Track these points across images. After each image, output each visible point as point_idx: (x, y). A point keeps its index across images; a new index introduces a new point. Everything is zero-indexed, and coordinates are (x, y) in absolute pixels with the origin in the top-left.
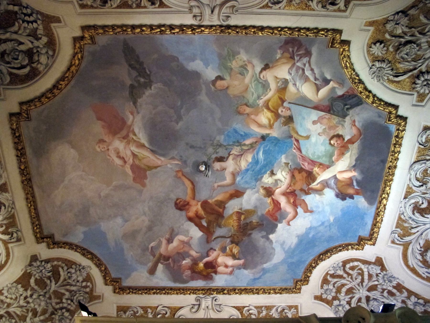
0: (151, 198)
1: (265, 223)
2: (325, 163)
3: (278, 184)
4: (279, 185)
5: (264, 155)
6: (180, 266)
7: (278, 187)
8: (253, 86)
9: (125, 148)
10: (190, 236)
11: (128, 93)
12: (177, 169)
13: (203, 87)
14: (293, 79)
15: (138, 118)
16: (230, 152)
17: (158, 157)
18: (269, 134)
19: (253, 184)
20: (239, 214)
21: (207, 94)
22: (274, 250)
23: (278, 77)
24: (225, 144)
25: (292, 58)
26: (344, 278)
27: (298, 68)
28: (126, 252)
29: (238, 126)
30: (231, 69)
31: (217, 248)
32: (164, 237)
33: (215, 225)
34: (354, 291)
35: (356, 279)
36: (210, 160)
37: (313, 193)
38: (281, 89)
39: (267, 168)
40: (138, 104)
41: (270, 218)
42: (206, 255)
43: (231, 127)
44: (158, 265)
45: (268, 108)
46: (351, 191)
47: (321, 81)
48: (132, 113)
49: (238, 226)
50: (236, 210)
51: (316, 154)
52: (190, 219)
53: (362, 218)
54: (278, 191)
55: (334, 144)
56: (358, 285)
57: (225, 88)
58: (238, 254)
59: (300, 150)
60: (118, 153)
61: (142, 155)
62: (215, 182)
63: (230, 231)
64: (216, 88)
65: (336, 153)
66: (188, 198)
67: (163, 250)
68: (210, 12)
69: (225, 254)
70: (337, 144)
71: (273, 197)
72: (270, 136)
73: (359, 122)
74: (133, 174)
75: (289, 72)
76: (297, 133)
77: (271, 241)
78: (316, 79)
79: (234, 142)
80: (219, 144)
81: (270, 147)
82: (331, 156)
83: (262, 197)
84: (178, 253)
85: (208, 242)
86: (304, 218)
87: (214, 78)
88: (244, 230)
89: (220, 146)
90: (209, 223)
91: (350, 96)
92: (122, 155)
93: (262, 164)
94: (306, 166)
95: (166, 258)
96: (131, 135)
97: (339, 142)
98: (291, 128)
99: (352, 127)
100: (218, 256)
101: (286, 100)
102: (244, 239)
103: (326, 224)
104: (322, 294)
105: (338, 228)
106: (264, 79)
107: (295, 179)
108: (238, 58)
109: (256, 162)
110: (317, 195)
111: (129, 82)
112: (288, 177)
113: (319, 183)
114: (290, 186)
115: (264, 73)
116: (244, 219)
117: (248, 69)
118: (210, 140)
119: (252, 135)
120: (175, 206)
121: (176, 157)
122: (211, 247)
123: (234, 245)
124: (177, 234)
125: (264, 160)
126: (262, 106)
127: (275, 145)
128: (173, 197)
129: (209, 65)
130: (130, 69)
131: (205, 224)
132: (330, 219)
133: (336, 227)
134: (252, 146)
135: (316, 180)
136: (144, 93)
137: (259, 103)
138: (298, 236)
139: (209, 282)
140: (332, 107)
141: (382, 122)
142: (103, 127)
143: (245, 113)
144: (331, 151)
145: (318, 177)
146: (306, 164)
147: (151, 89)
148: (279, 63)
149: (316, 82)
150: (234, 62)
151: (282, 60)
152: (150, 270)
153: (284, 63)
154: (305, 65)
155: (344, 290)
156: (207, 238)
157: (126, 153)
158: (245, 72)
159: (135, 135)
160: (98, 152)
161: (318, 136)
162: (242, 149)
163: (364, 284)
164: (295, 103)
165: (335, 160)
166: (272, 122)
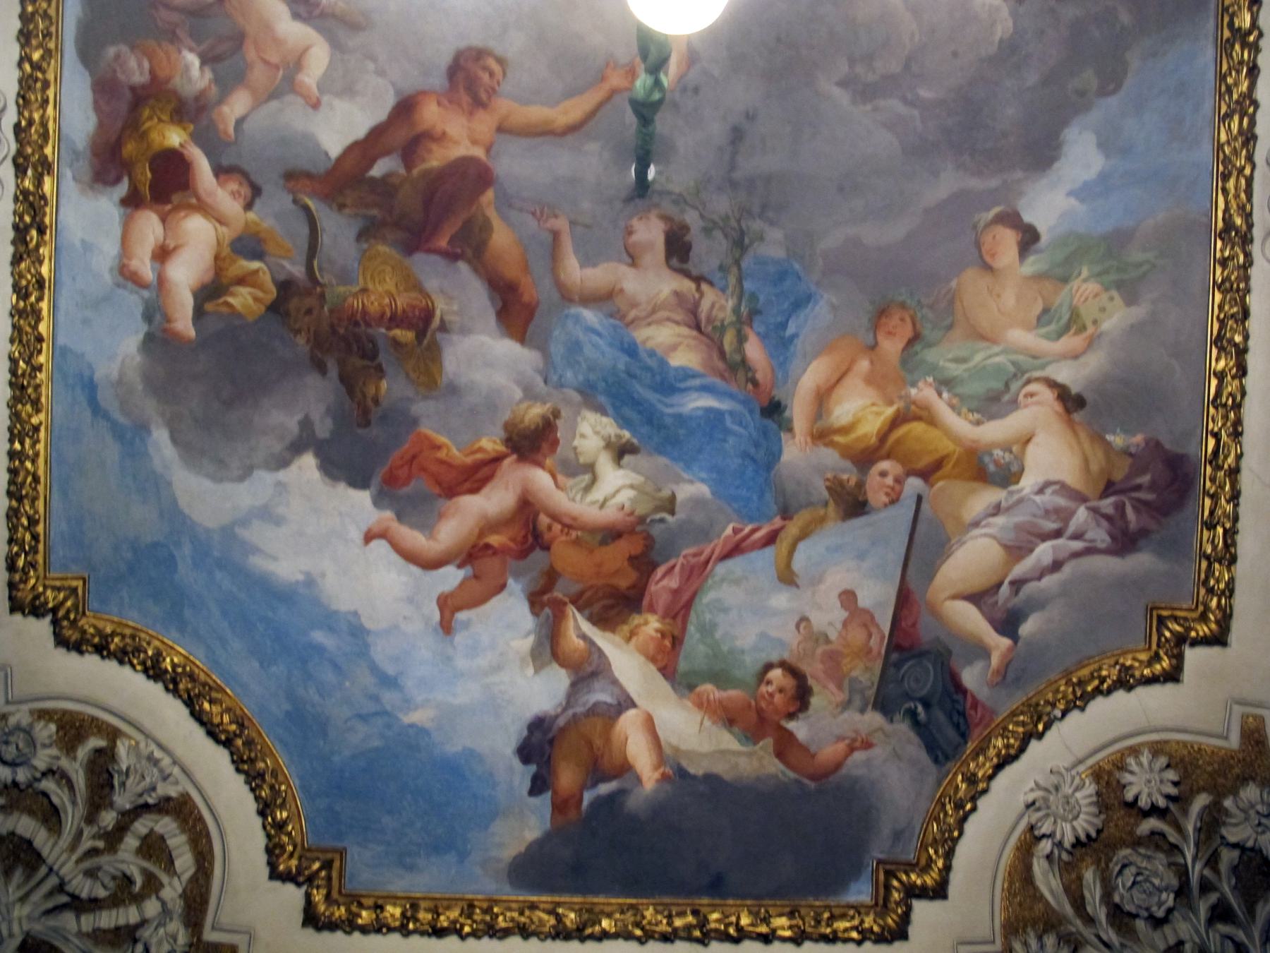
1: (375, 431)
4: (570, 482)
5: (700, 413)
6: (173, 38)
7: (560, 477)
8: (997, 359)
13: (994, 183)
14: (1020, 501)
16: (711, 284)
18: (790, 430)
19: (569, 374)
20: (422, 321)
22: (241, 479)
23: (1031, 448)
24: (746, 263)
25: (1109, 488)
26: (91, 819)
27: (1064, 515)
30: (1065, 280)
31: (262, 218)
33: (375, 212)
34: (18, 875)
35: (91, 874)
36: (675, 202)
38: (980, 460)
39: (645, 430)
42: (225, 162)
43: (818, 284)
45: (896, 422)
46: (567, 777)
47: (1010, 605)
49: (365, 312)
50: (440, 306)
52: (405, 108)
53: (438, 847)
54: (540, 479)
55: (769, 683)
56: (61, 888)
57: (988, 259)
59: (735, 550)
62: (573, 223)
63: (345, 277)
65: (733, 693)
66: (503, 105)
69: (226, 251)
70: (771, 695)
71: (507, 462)
73: (868, 763)
75: (1048, 484)
76: (804, 535)
77: (282, 463)
78: (1017, 584)
79: (753, 297)
80: (747, 241)
81: (735, 434)
82: (720, 678)
83: (507, 416)
84: (239, 39)
85: (291, 176)
86: (410, 600)
87: (1027, 218)
89: (740, 243)
90: (385, 187)
91: (962, 714)
93: (660, 406)
94: (665, 582)
97: (778, 698)
98: (822, 512)
100: (221, 220)
102: (301, 340)
103: (389, 698)
105: (377, 749)
106: (1021, 397)
107: (604, 543)
108: (1112, 299)
109: (669, 383)
110: (531, 640)
112: (610, 515)
113: (591, 643)
114: (568, 527)
115: (1048, 395)
116: (396, 343)
117: (1064, 339)
118: (764, 207)
119: (782, 365)
120: (470, 49)
122: (267, 189)
123: (273, 292)
124: (336, 45)
127: (745, 455)
129: (1082, 201)
131: (377, 171)
132: (416, 708)
133: (377, 743)
134: (738, 367)
137: (921, 384)
138: (310, 582)
139: (84, 166)
140: (913, 657)
141: (878, 850)
143: (881, 338)
144: (738, 673)
145: (617, 638)
146: (673, 582)
148: (1087, 446)
149: (1005, 589)
150: (1092, 287)
153: (1086, 461)
154: (1077, 536)
155: (25, 825)
156: (309, 175)
158: (1053, 327)
161: (796, 619)
162: (722, 329)
163: (68, 921)
164: (922, 516)
165: (699, 695)
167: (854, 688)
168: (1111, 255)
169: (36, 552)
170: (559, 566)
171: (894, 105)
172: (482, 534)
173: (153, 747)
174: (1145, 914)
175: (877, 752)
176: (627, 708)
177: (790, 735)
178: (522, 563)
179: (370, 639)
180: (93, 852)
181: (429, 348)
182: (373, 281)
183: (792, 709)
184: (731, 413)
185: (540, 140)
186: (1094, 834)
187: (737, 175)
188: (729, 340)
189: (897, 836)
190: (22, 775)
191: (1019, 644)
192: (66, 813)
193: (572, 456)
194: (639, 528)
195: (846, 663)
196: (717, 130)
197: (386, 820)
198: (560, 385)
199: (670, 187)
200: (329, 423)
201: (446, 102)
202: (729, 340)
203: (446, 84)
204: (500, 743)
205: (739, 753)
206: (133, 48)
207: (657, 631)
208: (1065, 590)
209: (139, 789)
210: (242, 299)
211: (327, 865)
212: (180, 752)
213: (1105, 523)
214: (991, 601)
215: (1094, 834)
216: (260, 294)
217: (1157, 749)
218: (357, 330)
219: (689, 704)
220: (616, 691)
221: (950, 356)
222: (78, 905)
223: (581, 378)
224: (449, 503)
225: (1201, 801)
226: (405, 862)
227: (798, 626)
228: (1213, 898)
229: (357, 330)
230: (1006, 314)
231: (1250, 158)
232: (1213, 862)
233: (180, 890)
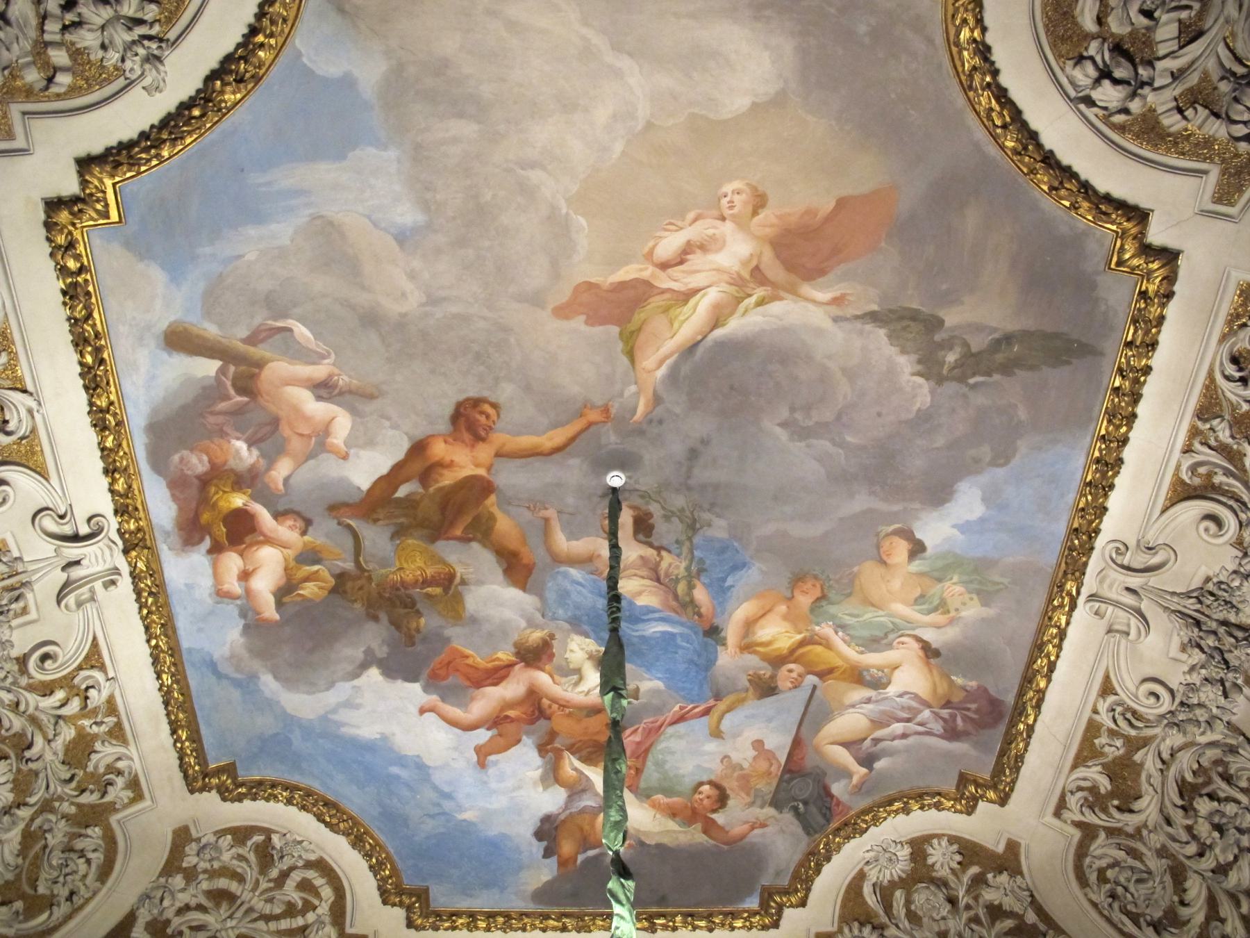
0: (506, 329)
1: (419, 647)
3: (566, 676)
4: (564, 680)
6: (223, 434)
7: (556, 677)
10: (352, 451)
12: (613, 411)
13: (896, 508)
15: (819, 317)
16: (669, 551)
17: (669, 362)
18: (724, 645)
20: (448, 581)
21: (870, 511)
22: (328, 689)
23: (897, 673)
24: (697, 539)
25: (948, 704)
28: (252, 231)
29: (753, 575)
30: (940, 580)
32: (336, 371)
33: (402, 520)
35: (270, 900)
36: (642, 497)
37: (546, 763)
40: (868, 327)
41: (438, 659)
42: (281, 508)
44: (212, 357)
45: (802, 643)
46: (567, 848)
48: (837, 301)
49: (403, 582)
50: (460, 571)
51: (668, 758)
52: (418, 448)
53: (487, 885)
54: (542, 678)
57: (885, 558)
58: (299, 599)
59: (681, 719)
60: (703, 248)
61: (682, 318)
63: (384, 563)
64: (888, 535)
65: (675, 799)
66: (500, 438)
67: (278, 368)
69: (292, 564)
71: (517, 667)
72: (719, 648)
73: (763, 835)
74: (611, 284)
75: (906, 693)
76: (730, 709)
77: (355, 675)
78: (876, 741)
79: (701, 561)
80: (698, 526)
81: (683, 648)
82: (667, 792)
83: (516, 637)
84: (275, 422)
85: (334, 508)
86: (456, 749)
87: (918, 535)
88: (389, 599)
89: (693, 527)
90: (410, 503)
91: (830, 809)
92: (696, 260)
93: (628, 631)
96: (760, 292)
100: (282, 545)
102: (358, 606)
103: (447, 805)
104: (198, 840)
107: (588, 716)
110: (540, 771)
111: (952, 318)
113: (582, 773)
116: (429, 596)
119: (721, 604)
120: (467, 400)
121: (659, 410)
123: (332, 582)
124: (353, 411)
125: (642, 638)
126: (813, 630)
127: (691, 662)
128: (506, 393)
129: (962, 533)
130: (996, 336)
131: (402, 492)
133: (442, 830)
134: (688, 605)
139: (175, 539)
142: (810, 212)
143: (797, 593)
146: (637, 738)
147: (913, 374)
148: (937, 679)
149: (868, 742)
150: (958, 589)
151: (945, 685)
152: (186, 330)
156: (346, 505)
157: (698, 271)
159: (761, 303)
160: (720, 186)
162: (677, 581)
163: (261, 925)
164: (815, 697)
166: (758, 649)
167: (758, 794)
171: (823, 445)
172: (502, 709)
177: (713, 821)
178: (533, 727)
179: (431, 771)
184: (681, 635)
187: (691, 482)
189: (778, 874)
193: (564, 663)
196: (677, 448)
198: (554, 619)
199: (637, 487)
200: (385, 649)
201: (450, 440)
202: (681, 588)
204: (523, 831)
206: (192, 450)
208: (907, 750)
213: (941, 722)
214: (856, 747)
217: (952, 840)
223: (569, 614)
224: (477, 692)
225: (974, 870)
226: (466, 892)
228: (972, 913)
229: (399, 593)
230: (893, 590)
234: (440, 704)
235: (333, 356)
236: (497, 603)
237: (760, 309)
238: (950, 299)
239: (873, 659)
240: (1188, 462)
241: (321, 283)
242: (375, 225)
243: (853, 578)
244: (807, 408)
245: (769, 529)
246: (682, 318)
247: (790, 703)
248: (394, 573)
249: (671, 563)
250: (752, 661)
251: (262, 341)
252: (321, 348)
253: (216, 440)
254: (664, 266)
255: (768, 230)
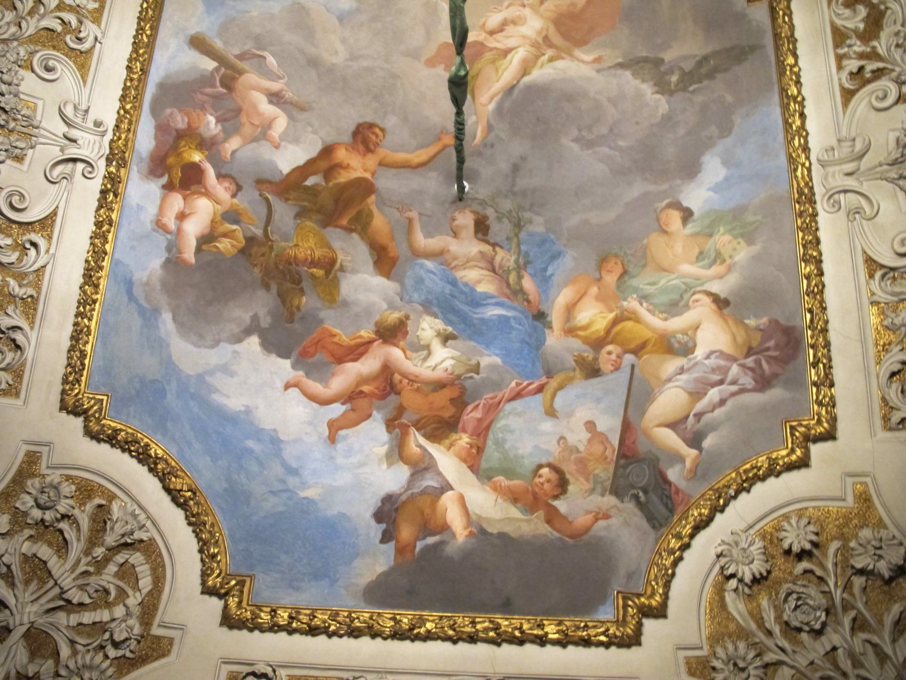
0: (395, 76)
1: (296, 326)
2: (483, 458)
3: (417, 351)
4: (414, 355)
6: (203, 108)
7: (408, 352)
9: (524, 37)
10: (283, 144)
11: (644, 54)
13: (665, 187)
14: (696, 364)
15: (587, 71)
16: (502, 247)
17: (497, 99)
18: (551, 328)
19: (416, 296)
20: (330, 265)
21: (646, 195)
22: (212, 347)
24: (523, 235)
26: (87, 552)
27: (725, 371)
29: (567, 262)
30: (711, 235)
32: (286, 88)
33: (305, 204)
34: (33, 586)
35: (82, 588)
36: (480, 204)
38: (669, 342)
39: (462, 326)
40: (620, 72)
42: (223, 172)
43: (565, 246)
44: (214, 59)
45: (615, 322)
46: (406, 532)
47: (695, 429)
48: (598, 60)
49: (296, 257)
50: (341, 257)
52: (327, 151)
53: (317, 576)
54: (396, 353)
55: (540, 476)
58: (215, 250)
59: (517, 395)
60: (514, 22)
61: (503, 67)
63: (286, 238)
64: (662, 210)
66: (382, 152)
67: (251, 78)
68: (846, 172)
69: (219, 218)
70: (542, 484)
71: (376, 343)
72: (547, 331)
73: (608, 528)
76: (561, 387)
77: (239, 340)
78: (699, 416)
79: (527, 254)
80: (522, 224)
81: (517, 330)
82: (509, 473)
83: (378, 317)
84: (238, 111)
85: (260, 182)
86: (310, 423)
87: (685, 204)
88: (283, 272)
89: (518, 225)
90: (313, 191)
91: (669, 497)
92: (510, 29)
93: (471, 314)
94: (472, 414)
95: (229, 83)
96: (550, 53)
98: (572, 374)
99: (591, 512)
101: (639, 358)
102: (257, 270)
103: (292, 481)
106: (690, 303)
107: (435, 390)
108: (739, 243)
109: (477, 301)
110: (386, 447)
111: (668, 56)
112: (439, 374)
113: (425, 450)
116: (313, 276)
117: (714, 267)
118: (532, 205)
120: (365, 123)
121: (492, 136)
122: (245, 187)
124: (291, 117)
126: (622, 306)
127: (523, 341)
128: (390, 122)
129: (716, 193)
130: (698, 58)
131: (310, 182)
132: (309, 487)
134: (518, 292)
135: (433, 442)
136: (644, 81)
137: (629, 299)
138: (248, 411)
139: (145, 167)
140: (635, 462)
143: (604, 273)
145: (442, 448)
146: (478, 414)
147: (653, 93)
148: (733, 328)
149: (691, 419)
150: (727, 238)
151: (743, 333)
154: (734, 383)
155: (44, 551)
156: (270, 182)
157: (512, 36)
158: (706, 262)
159: (551, 60)
161: (557, 438)
162: (508, 272)
163: (61, 618)
164: (635, 377)
165: (495, 483)
168: (735, 219)
169: (82, 376)
170: (405, 404)
171: (605, 150)
172: (358, 384)
173: (136, 507)
174: (807, 628)
175: (613, 521)
176: (447, 490)
177: (555, 509)
179: (282, 446)
180: (86, 573)
181: (331, 281)
182: (302, 242)
183: (556, 493)
184: (515, 318)
185: (402, 170)
186: (765, 574)
187: (516, 189)
188: (512, 278)
189: (630, 576)
190: (49, 516)
191: (704, 452)
192: (72, 547)
193: (416, 340)
194: (456, 382)
195: (591, 465)
196: (504, 166)
197: (284, 557)
198: (410, 301)
199: (477, 196)
200: (269, 320)
201: (350, 148)
202: (512, 278)
203: (351, 140)
204: (362, 511)
205: (522, 520)
206: (180, 111)
207: (467, 443)
208: (729, 417)
209: (122, 532)
210: (224, 245)
211: (241, 583)
212: (152, 510)
213: (750, 373)
215: (765, 574)
216: (235, 243)
218: (290, 267)
219: (488, 488)
220: (440, 479)
221: (646, 282)
222: (69, 606)
223: (423, 297)
226: (293, 585)
227: (558, 442)
228: (853, 613)
229: (290, 267)
230: (678, 257)
231: (808, 158)
232: (848, 587)
233: (140, 600)
234: (304, 380)
235: (286, 79)
236: (366, 289)
237: (550, 64)
238: (665, 46)
239: (676, 324)
240: (844, 75)
241: (289, 37)
242: (328, 10)
243: (645, 249)
244: (590, 128)
245: (574, 221)
246: (503, 67)
247: (615, 383)
248: (291, 248)
249: (502, 257)
250: (575, 344)
251: (247, 59)
252: (281, 73)
253: (198, 111)
254: (492, 33)
255: (550, 14)
